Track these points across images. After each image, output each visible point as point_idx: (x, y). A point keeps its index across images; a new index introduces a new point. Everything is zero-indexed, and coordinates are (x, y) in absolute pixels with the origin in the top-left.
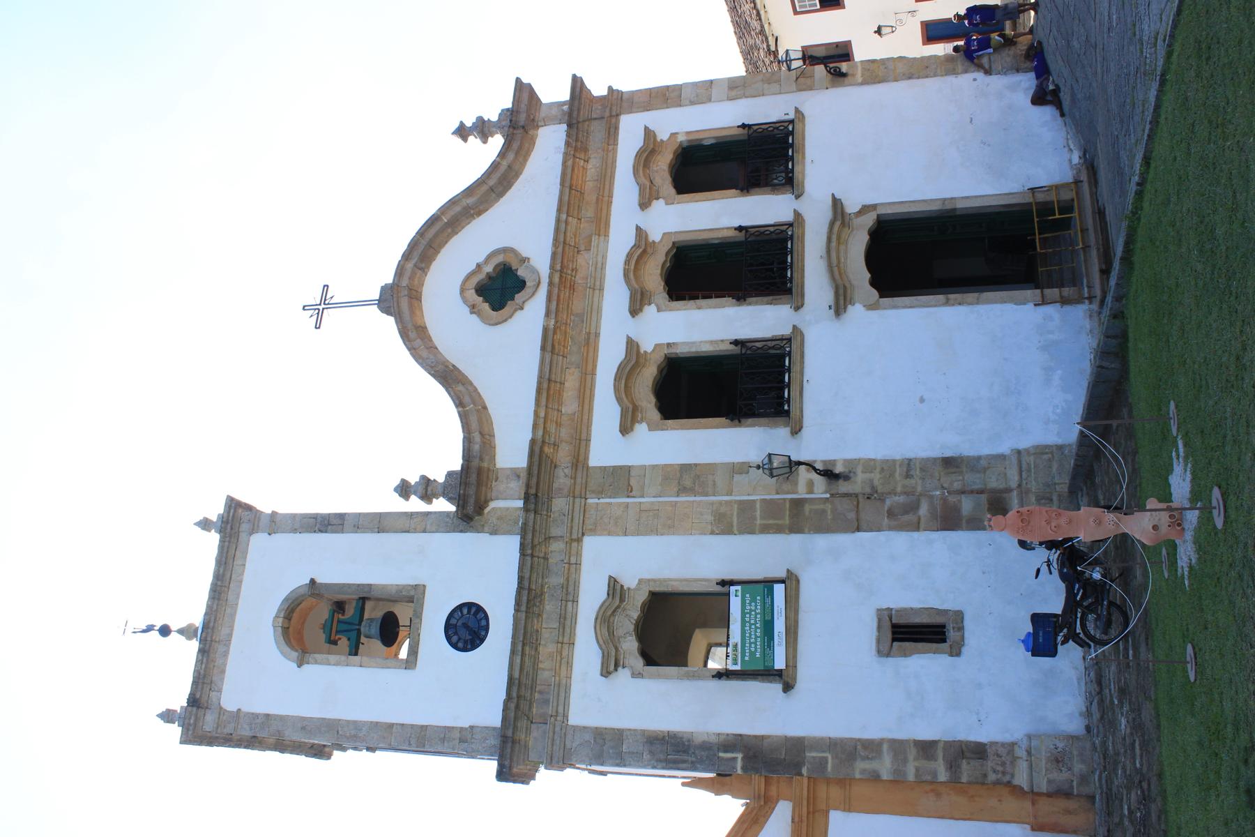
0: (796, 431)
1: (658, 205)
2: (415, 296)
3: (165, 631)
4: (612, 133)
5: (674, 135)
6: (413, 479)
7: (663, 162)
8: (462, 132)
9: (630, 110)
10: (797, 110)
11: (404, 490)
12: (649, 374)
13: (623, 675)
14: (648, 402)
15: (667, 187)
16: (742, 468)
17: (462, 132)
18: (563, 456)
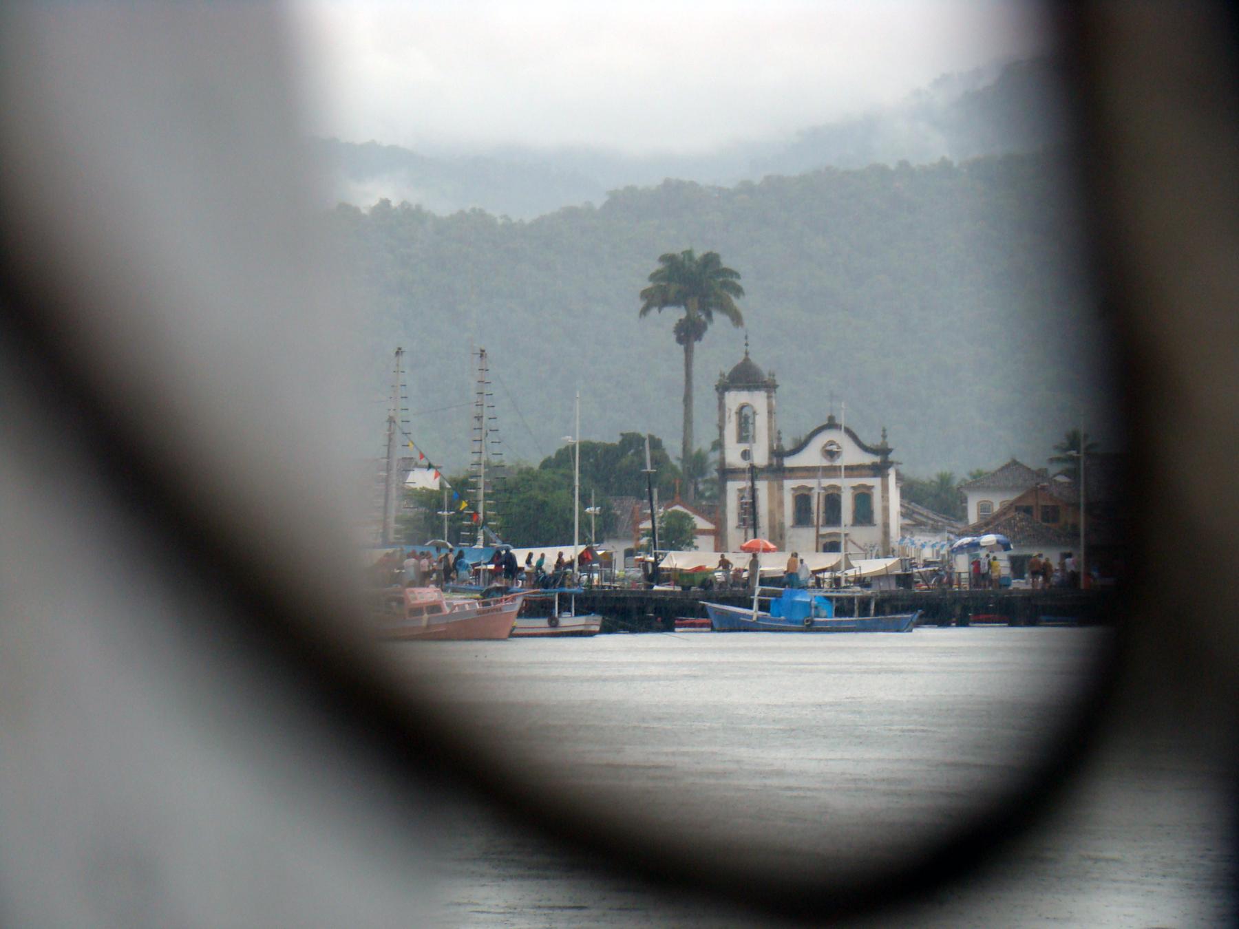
0: (793, 527)
1: (852, 491)
2: (829, 428)
3: (747, 345)
4: (875, 476)
5: (872, 493)
6: (781, 435)
7: (865, 491)
8: (884, 430)
9: (882, 481)
10: (875, 525)
11: (779, 433)
12: (806, 493)
13: (738, 493)
14: (799, 493)
15: (856, 493)
16: (783, 516)
17: (884, 430)
18: (787, 474)
